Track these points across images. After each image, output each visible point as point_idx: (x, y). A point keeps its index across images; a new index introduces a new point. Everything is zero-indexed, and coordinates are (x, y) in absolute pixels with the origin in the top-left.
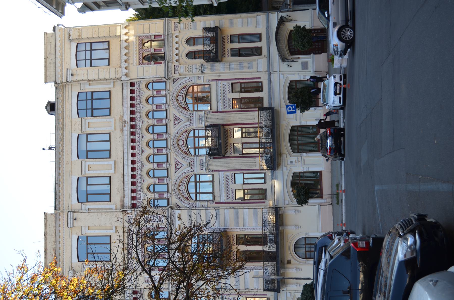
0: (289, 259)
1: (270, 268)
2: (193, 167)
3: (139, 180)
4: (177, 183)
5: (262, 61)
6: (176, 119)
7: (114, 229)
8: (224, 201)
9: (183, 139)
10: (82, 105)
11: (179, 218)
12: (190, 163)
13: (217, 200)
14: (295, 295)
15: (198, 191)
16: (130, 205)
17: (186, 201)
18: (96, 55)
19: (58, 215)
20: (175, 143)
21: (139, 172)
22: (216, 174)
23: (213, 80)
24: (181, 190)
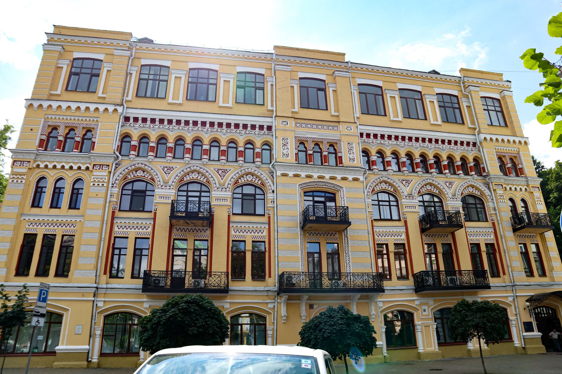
0: (315, 307)
1: (303, 282)
2: (407, 198)
3: (387, 143)
4: (389, 180)
5: (520, 276)
6: (451, 183)
7: (337, 114)
8: (374, 230)
9: (432, 189)
10: (447, 99)
11: (355, 180)
12: (411, 194)
13: (375, 223)
14: (269, 313)
15: (381, 203)
16: (362, 131)
17: (371, 189)
18: (493, 114)
19: (345, 64)
20: (429, 181)
21: (395, 143)
22: (402, 223)
23: (494, 224)
24: (382, 185)
